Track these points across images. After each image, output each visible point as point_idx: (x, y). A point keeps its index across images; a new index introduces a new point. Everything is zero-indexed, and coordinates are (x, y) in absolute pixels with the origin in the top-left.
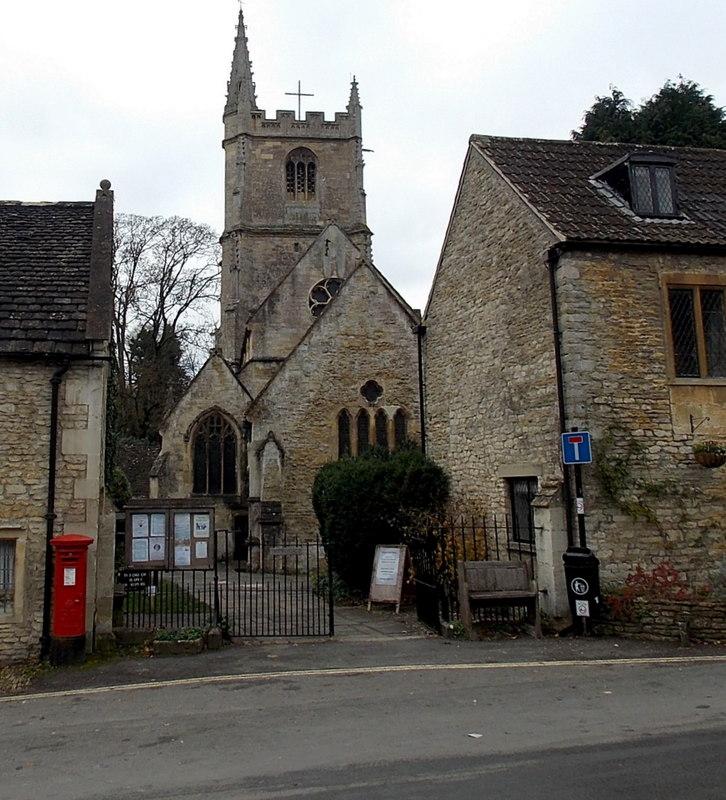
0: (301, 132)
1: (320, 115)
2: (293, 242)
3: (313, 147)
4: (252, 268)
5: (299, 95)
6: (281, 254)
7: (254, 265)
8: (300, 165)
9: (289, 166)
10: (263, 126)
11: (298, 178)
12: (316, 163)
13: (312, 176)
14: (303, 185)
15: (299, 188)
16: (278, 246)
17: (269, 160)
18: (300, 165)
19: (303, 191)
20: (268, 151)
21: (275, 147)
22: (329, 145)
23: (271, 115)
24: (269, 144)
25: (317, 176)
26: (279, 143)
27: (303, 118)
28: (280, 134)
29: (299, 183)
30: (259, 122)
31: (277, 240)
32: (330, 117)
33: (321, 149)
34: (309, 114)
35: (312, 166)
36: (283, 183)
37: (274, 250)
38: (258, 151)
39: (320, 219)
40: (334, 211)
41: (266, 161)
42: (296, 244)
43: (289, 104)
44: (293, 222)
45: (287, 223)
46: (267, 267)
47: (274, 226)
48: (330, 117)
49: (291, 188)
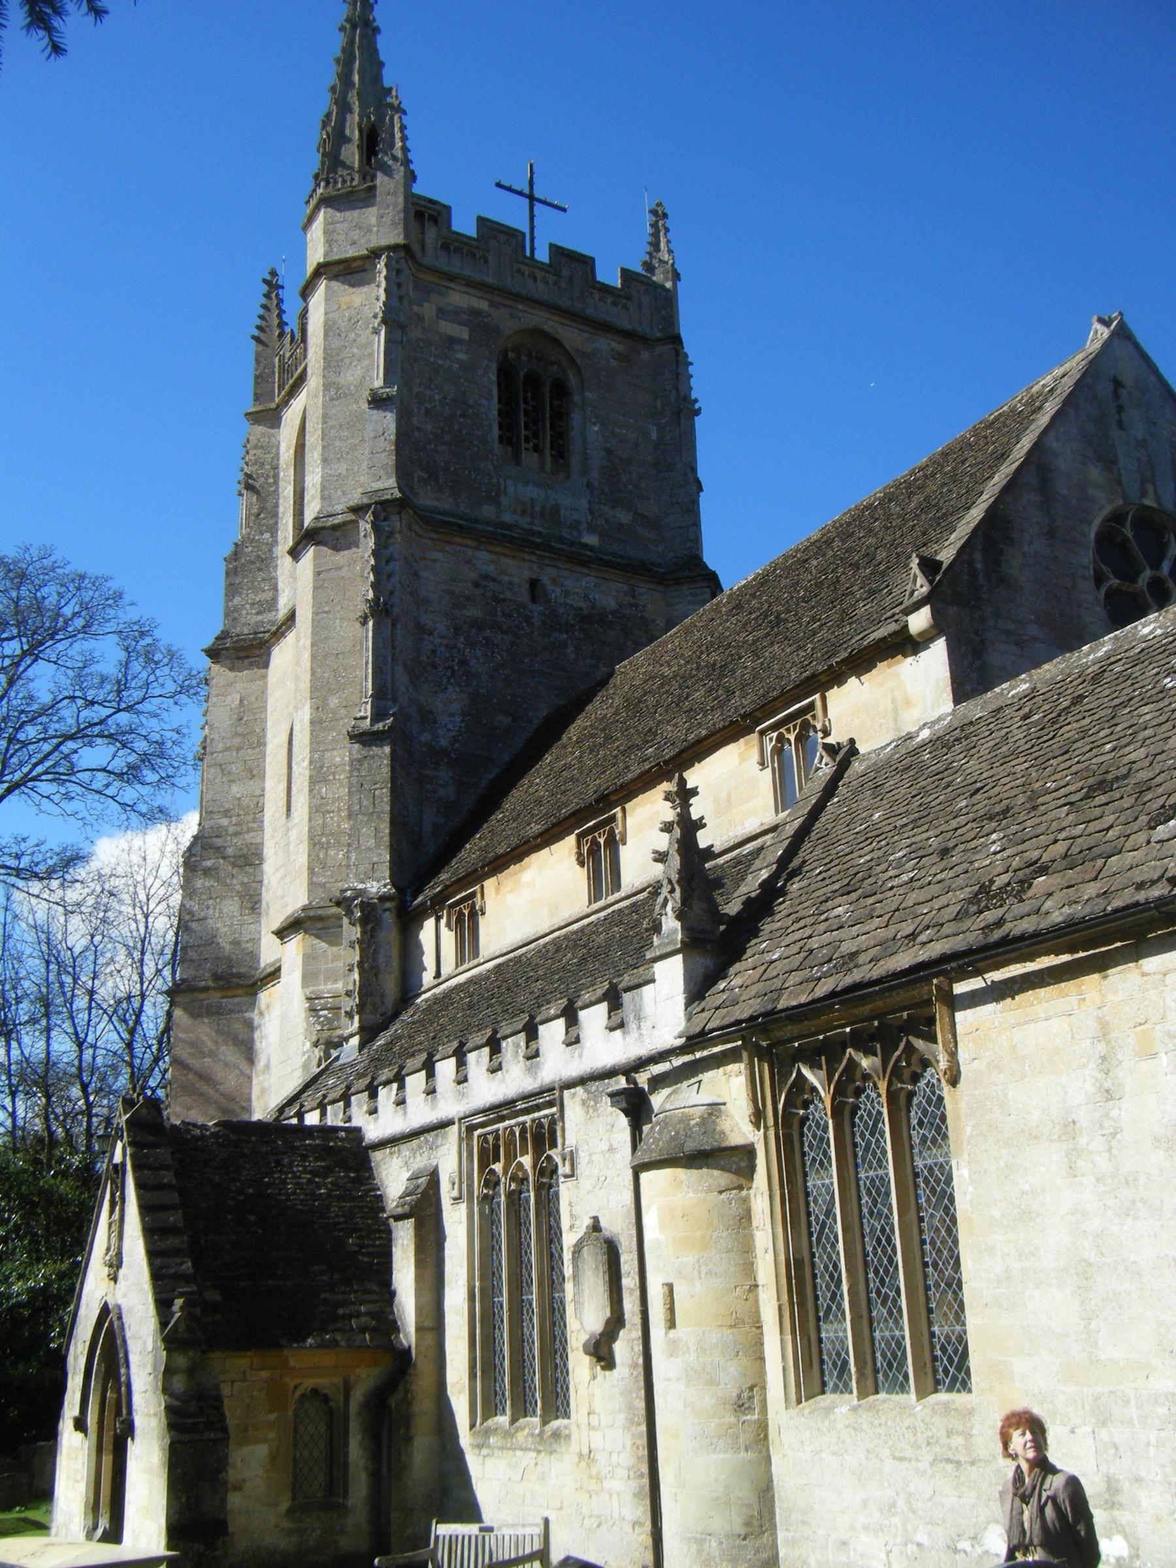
0: (539, 290)
1: (587, 262)
2: (526, 574)
3: (571, 336)
4: (420, 627)
5: (531, 198)
6: (496, 599)
7: (427, 620)
8: (533, 381)
9: (506, 374)
10: (446, 247)
11: (526, 413)
12: (573, 381)
13: (560, 417)
14: (536, 435)
15: (527, 440)
16: (486, 577)
17: (459, 341)
18: (533, 381)
19: (536, 449)
20: (455, 315)
21: (475, 312)
22: (606, 345)
23: (464, 224)
24: (458, 298)
25: (576, 418)
26: (484, 305)
27: (543, 255)
28: (490, 280)
29: (527, 427)
30: (431, 234)
31: (484, 559)
32: (609, 275)
33: (589, 348)
34: (557, 251)
35: (560, 390)
36: (491, 409)
37: (476, 585)
38: (428, 310)
39: (592, 529)
40: (624, 517)
41: (451, 341)
42: (534, 584)
43: (513, 214)
44: (524, 522)
45: (507, 518)
46: (457, 629)
47: (476, 521)
48: (609, 275)
49: (508, 436)
